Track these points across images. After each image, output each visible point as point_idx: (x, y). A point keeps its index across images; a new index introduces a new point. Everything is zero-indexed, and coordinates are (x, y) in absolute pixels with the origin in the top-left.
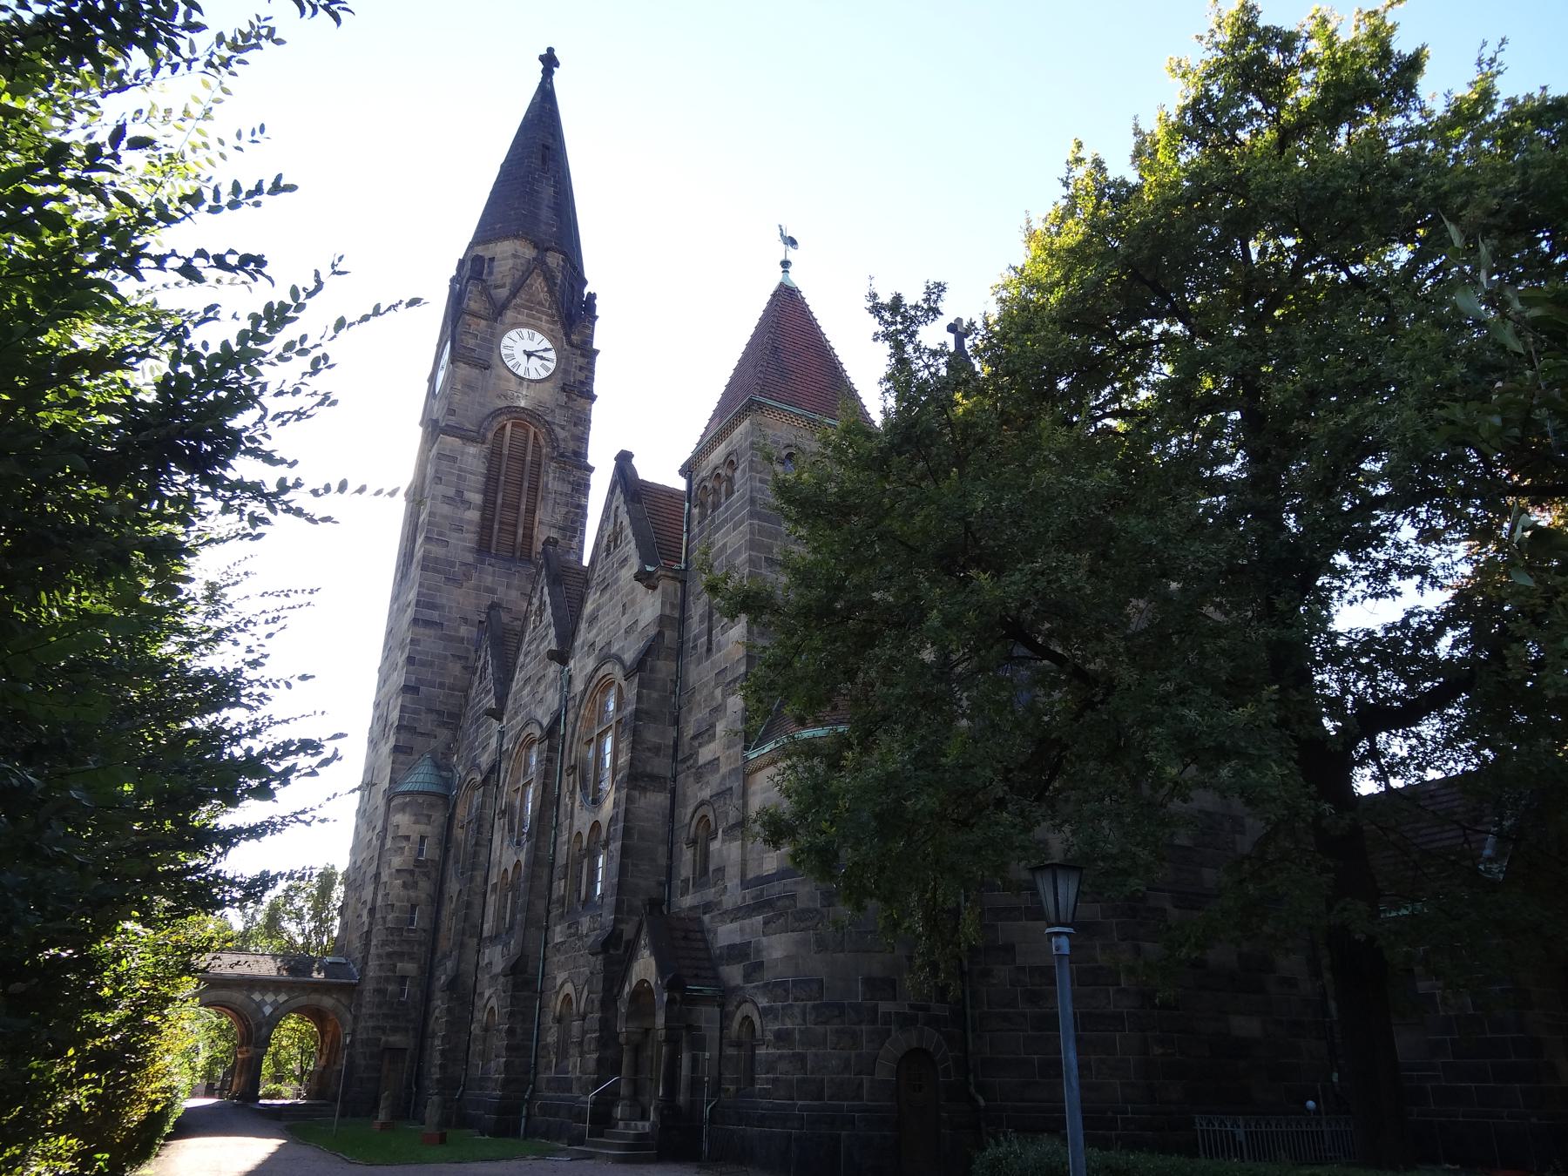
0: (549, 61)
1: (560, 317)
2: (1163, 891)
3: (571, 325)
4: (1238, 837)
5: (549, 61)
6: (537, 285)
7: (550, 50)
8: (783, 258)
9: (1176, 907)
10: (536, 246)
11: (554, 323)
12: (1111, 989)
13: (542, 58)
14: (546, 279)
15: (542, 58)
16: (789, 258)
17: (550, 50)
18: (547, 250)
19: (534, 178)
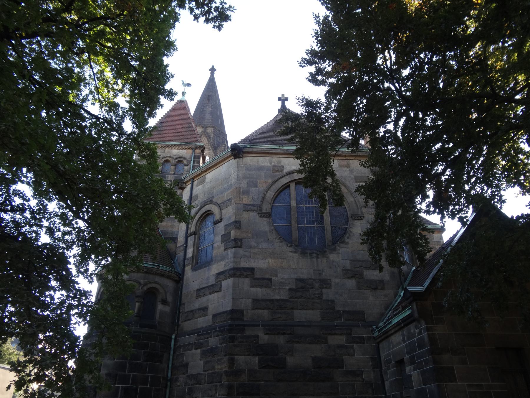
0: (213, 70)
1: (212, 148)
2: (258, 325)
3: (216, 150)
4: (324, 291)
5: (213, 70)
6: (204, 139)
7: (213, 67)
8: (183, 91)
9: (267, 334)
10: (203, 127)
11: (210, 150)
12: (218, 384)
13: (210, 70)
14: (206, 137)
15: (210, 70)
16: (185, 91)
17: (213, 67)
18: (207, 128)
19: (204, 107)
